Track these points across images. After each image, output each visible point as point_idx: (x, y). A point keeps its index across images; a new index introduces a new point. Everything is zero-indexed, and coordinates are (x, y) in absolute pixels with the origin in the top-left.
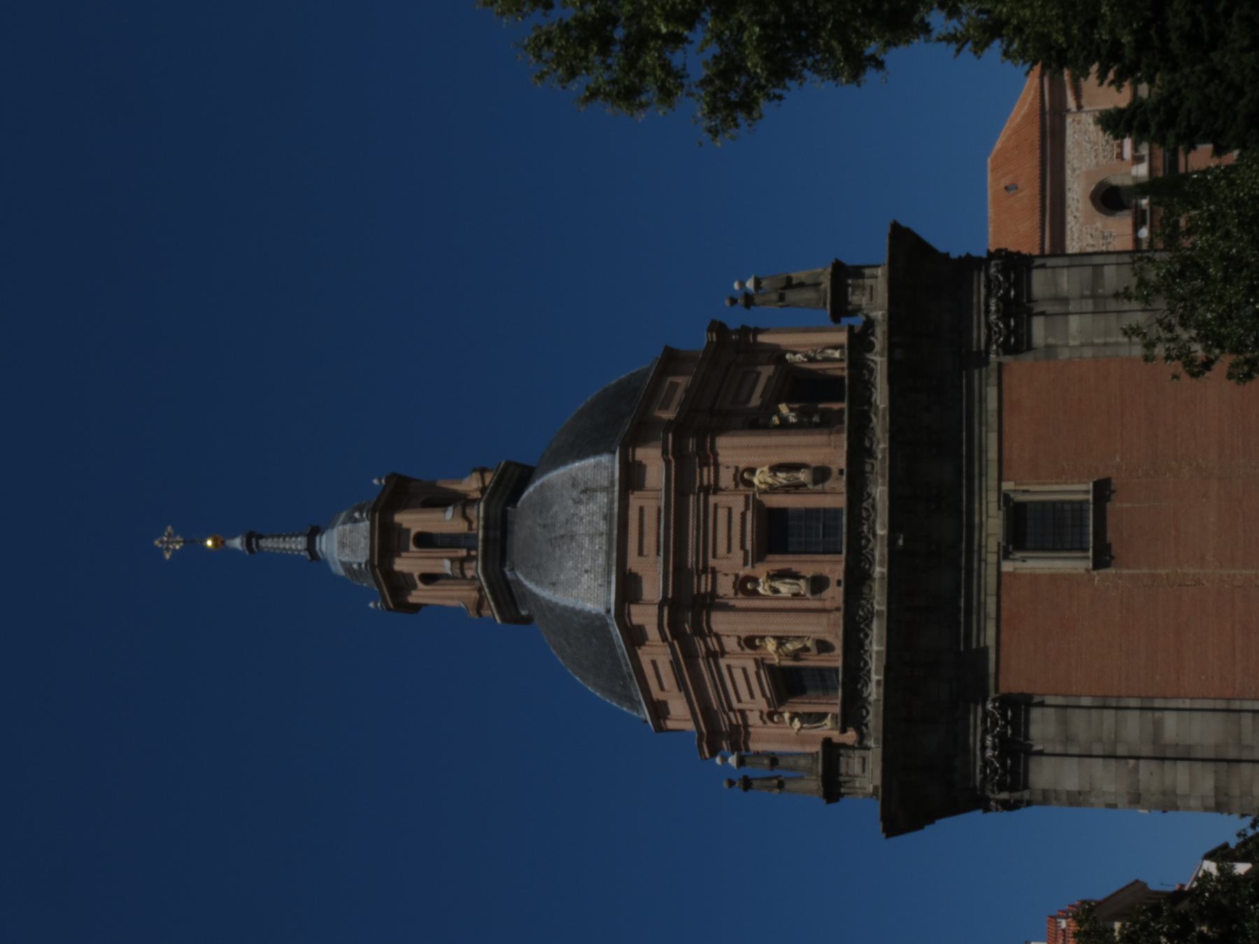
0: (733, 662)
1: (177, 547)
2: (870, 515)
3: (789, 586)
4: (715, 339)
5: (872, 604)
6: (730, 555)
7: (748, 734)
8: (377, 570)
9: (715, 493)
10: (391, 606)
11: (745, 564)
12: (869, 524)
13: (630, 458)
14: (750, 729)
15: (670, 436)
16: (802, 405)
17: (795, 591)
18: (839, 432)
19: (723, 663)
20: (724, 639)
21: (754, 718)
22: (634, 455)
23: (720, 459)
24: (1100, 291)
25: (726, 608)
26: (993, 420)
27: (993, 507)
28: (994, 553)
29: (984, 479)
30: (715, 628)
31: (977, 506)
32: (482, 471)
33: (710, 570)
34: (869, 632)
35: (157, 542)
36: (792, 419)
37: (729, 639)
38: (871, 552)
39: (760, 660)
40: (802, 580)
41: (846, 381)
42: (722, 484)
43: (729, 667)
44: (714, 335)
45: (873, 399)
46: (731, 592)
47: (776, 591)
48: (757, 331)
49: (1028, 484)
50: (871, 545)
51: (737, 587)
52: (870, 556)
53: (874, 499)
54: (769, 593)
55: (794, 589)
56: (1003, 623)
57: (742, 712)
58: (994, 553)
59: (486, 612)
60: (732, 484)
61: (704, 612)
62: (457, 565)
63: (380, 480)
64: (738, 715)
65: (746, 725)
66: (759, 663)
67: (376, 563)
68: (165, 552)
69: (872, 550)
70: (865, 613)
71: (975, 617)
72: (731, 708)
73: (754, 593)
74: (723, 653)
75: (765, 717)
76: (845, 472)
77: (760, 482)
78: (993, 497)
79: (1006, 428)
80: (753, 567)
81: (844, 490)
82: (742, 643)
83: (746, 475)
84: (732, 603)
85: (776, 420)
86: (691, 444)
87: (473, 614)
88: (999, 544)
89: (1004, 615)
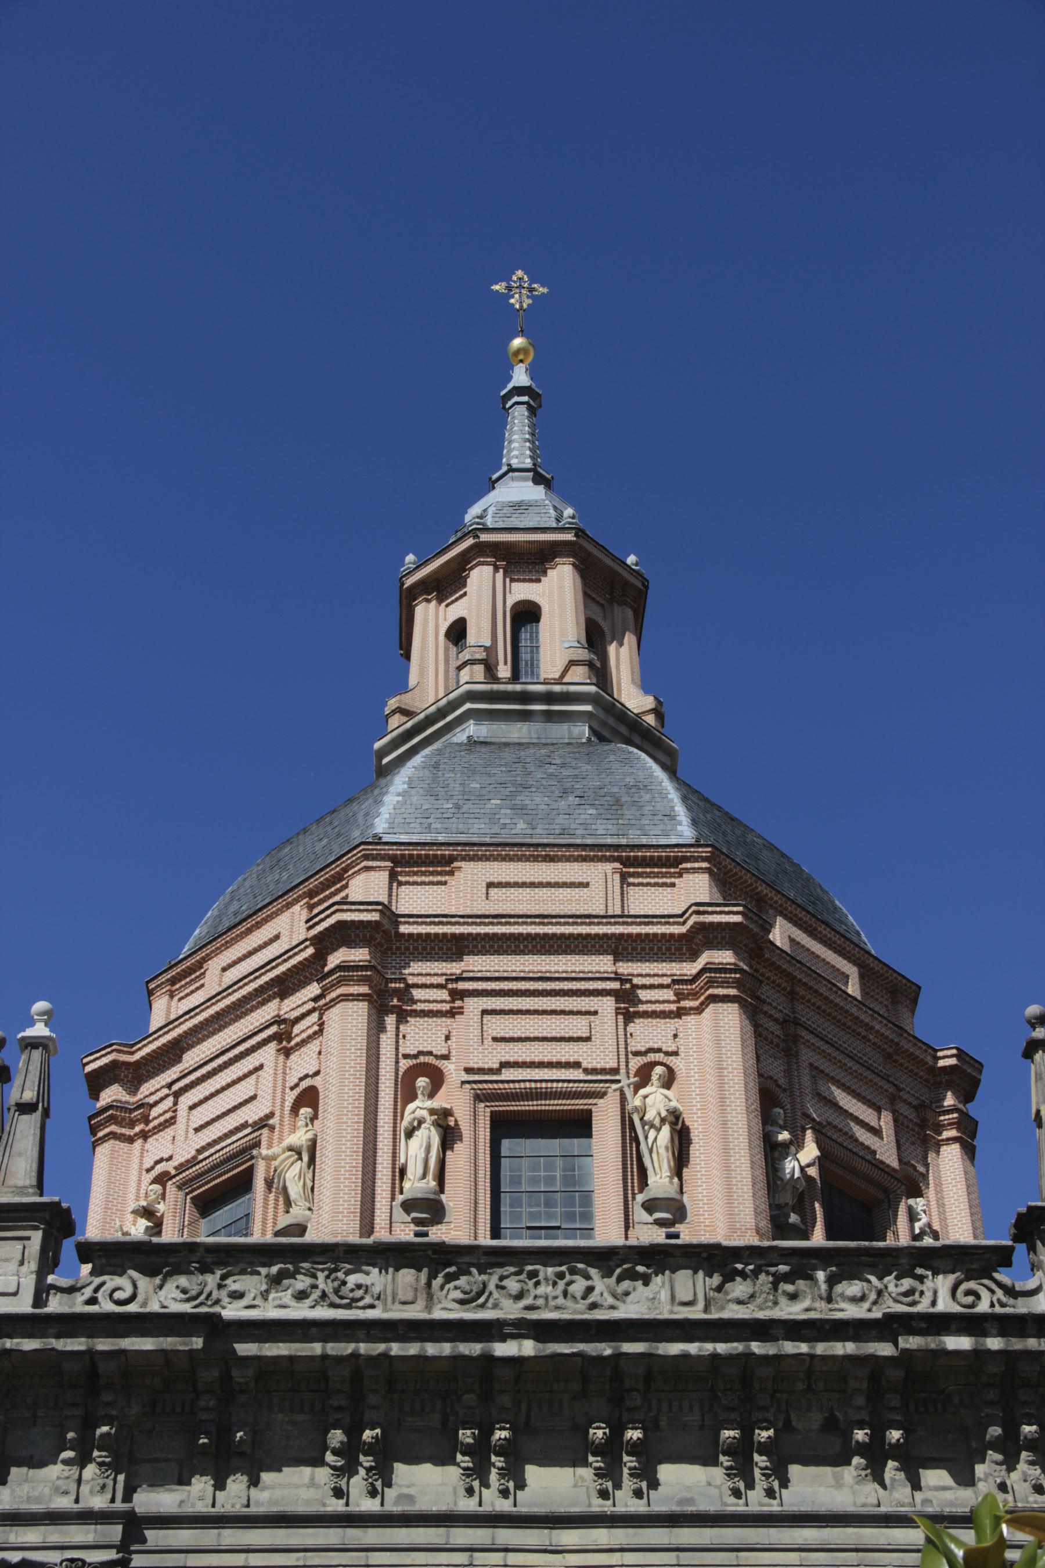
0: (266, 1074)
1: (512, 301)
2: (577, 1302)
3: (422, 1155)
4: (941, 1063)
5: (372, 1306)
6: (488, 1041)
7: (130, 1140)
8: (470, 542)
9: (618, 1012)
10: (409, 582)
11: (468, 1070)
12: (555, 1298)
13: (689, 865)
14: (139, 1143)
15: (737, 918)
16: (819, 1182)
17: (410, 1173)
18: (758, 1231)
19: (268, 1055)
20: (314, 1047)
21: (158, 1146)
22: (695, 870)
23: (690, 1020)
25: (377, 1028)
30: (333, 1016)
32: (657, 712)
33: (458, 1003)
34: (309, 1302)
35: (520, 273)
36: (791, 1166)
37: (315, 1055)
38: (491, 1301)
39: (271, 1122)
40: (433, 1184)
41: (881, 1244)
42: (638, 1027)
43: (261, 1066)
44: (953, 1061)
45: (843, 1305)
47: (410, 1134)
48: (970, 1151)
50: (507, 1303)
51: (422, 1059)
52: (481, 1300)
53: (612, 1307)
54: (408, 1118)
55: (414, 1170)
57: (171, 1122)
59: (395, 721)
60: (636, 1045)
61: (364, 989)
62: (481, 655)
63: (637, 564)
64: (168, 1116)
65: (145, 1136)
66: (262, 1123)
67: (484, 537)
68: (504, 284)
69: (496, 1306)
70: (352, 1290)
72: (177, 1095)
73: (407, 1093)
74: (287, 1053)
75: (160, 1168)
76: (673, 1241)
77: (645, 1097)
80: (463, 1083)
81: (632, 1242)
82: (304, 1084)
83: (659, 1070)
84: (387, 1041)
85: (784, 1136)
86: (726, 957)
87: (393, 703)
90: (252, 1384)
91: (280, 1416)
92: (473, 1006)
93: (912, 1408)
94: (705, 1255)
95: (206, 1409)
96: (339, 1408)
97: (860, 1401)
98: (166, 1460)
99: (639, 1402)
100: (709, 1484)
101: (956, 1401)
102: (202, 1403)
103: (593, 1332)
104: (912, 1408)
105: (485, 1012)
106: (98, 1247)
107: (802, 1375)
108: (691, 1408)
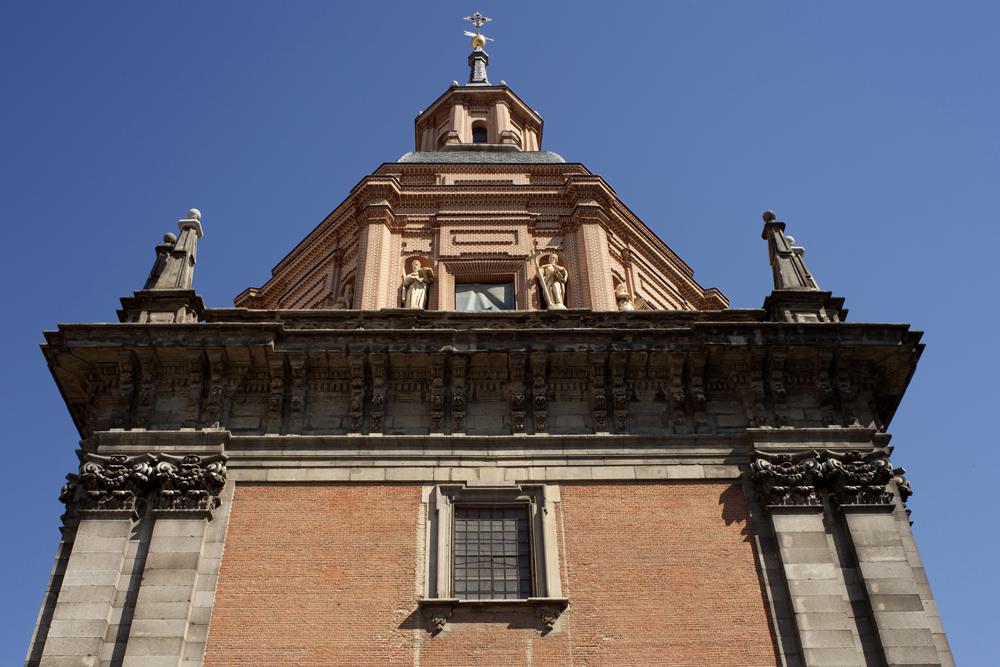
0: (329, 280)
24: (882, 606)
26: (654, 473)
27: (522, 475)
28: (450, 476)
29: (564, 462)
31: (521, 453)
43: (327, 275)
46: (409, 249)
49: (557, 517)
56: (344, 489)
58: (450, 476)
71: (353, 453)
78: (536, 474)
79: (641, 490)
88: (465, 482)
89: (354, 491)
90: (304, 372)
91: (322, 394)
92: (445, 231)
93: (709, 386)
94: (582, 319)
95: (276, 388)
96: (357, 387)
97: (678, 381)
98: (252, 416)
99: (543, 382)
100: (586, 427)
101: (735, 380)
102: (273, 384)
103: (514, 339)
104: (709, 386)
105: (452, 232)
106: (216, 315)
107: (643, 369)
108: (575, 388)
